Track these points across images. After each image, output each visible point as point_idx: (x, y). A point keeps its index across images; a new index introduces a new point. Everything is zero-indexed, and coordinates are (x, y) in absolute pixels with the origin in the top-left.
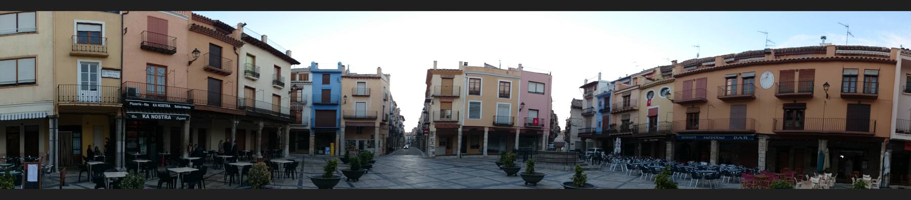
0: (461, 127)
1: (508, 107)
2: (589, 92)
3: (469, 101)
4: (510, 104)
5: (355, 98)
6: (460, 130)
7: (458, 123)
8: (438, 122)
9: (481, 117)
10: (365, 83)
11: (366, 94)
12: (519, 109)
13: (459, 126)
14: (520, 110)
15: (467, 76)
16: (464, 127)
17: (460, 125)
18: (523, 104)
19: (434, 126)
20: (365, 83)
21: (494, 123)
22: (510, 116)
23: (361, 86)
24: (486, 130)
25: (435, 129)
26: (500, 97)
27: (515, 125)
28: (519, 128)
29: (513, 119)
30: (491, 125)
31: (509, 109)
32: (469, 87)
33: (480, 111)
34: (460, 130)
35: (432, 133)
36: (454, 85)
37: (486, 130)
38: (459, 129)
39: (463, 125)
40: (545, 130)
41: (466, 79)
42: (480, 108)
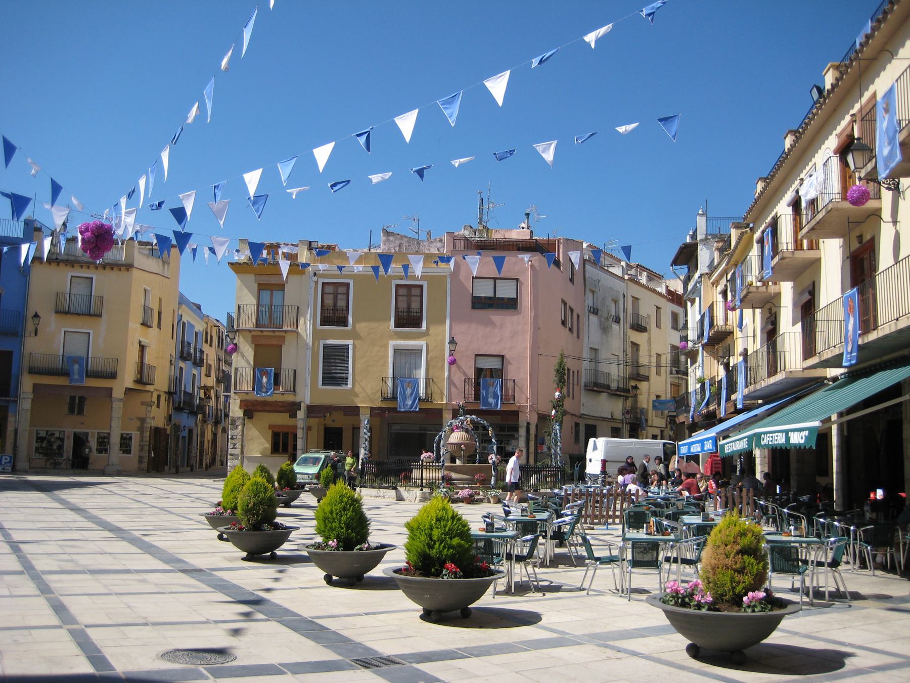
0: (303, 407)
15: (315, 279)
16: (312, 410)
17: (300, 403)
30: (378, 404)
39: (308, 402)
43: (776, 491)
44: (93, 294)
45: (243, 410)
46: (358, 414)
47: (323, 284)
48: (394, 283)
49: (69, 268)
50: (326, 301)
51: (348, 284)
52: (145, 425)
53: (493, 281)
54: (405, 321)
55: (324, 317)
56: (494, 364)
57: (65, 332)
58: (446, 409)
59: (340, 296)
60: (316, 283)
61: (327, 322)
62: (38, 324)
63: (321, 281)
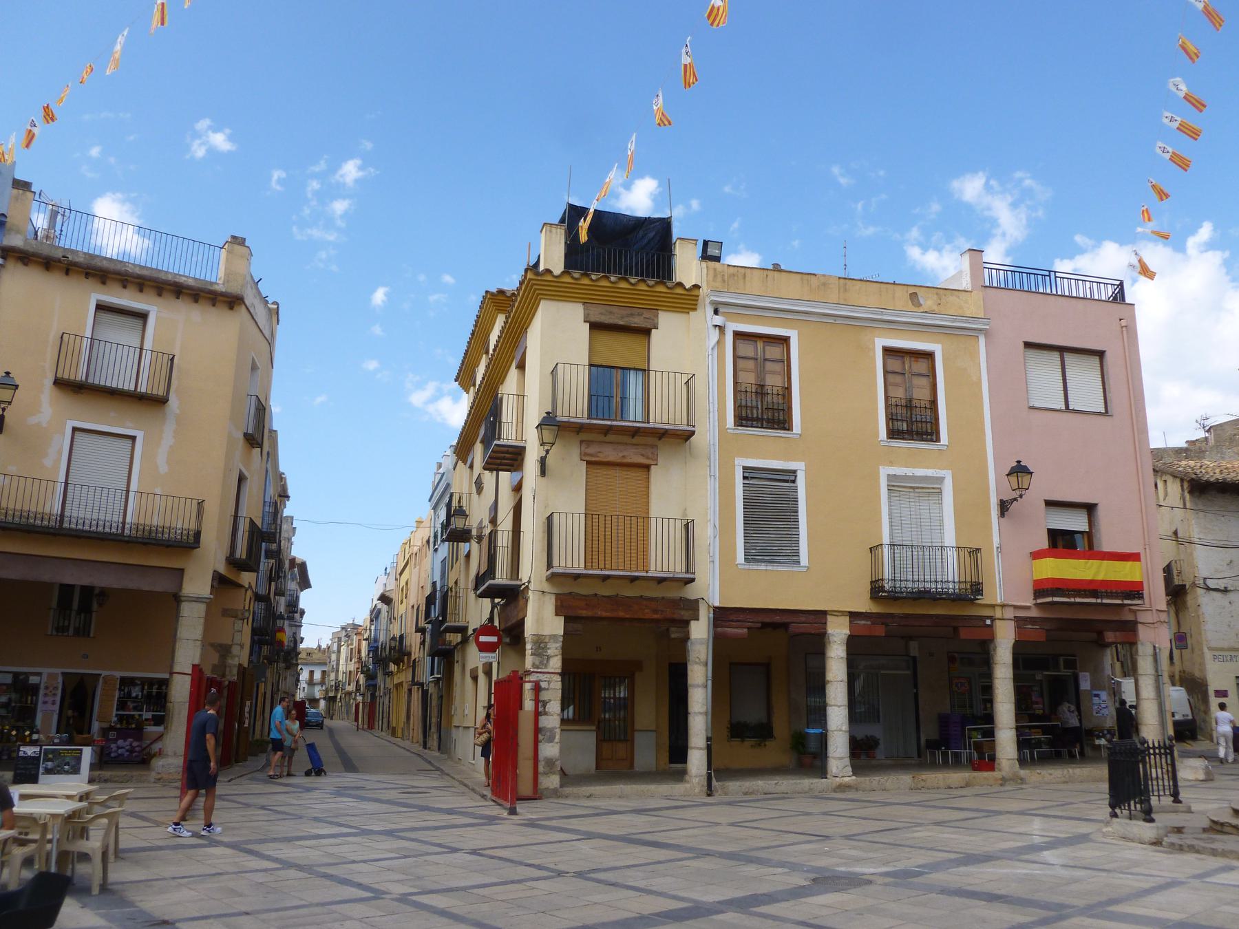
1: (929, 489)
3: (741, 462)
4: (948, 475)
5: (67, 402)
6: (700, 630)
7: (692, 592)
8: (577, 577)
10: (142, 316)
11: (142, 388)
13: (693, 607)
14: (1004, 507)
15: (718, 320)
16: (722, 615)
17: (697, 601)
18: (1020, 470)
19: (550, 604)
20: (142, 316)
21: (876, 590)
22: (950, 539)
23: (121, 334)
24: (838, 633)
25: (560, 621)
26: (893, 434)
27: (986, 599)
28: (1010, 614)
29: (976, 566)
30: (864, 605)
32: (736, 383)
34: (700, 630)
35: (540, 642)
37: (838, 633)
38: (693, 624)
40: (1142, 617)
41: (715, 336)
44: (148, 345)
45: (562, 618)
47: (738, 335)
48: (881, 342)
49: (89, 284)
51: (785, 341)
52: (230, 661)
53: (1056, 356)
55: (740, 406)
56: (1076, 522)
57: (75, 429)
61: (747, 419)
62: (10, 403)
63: (732, 327)
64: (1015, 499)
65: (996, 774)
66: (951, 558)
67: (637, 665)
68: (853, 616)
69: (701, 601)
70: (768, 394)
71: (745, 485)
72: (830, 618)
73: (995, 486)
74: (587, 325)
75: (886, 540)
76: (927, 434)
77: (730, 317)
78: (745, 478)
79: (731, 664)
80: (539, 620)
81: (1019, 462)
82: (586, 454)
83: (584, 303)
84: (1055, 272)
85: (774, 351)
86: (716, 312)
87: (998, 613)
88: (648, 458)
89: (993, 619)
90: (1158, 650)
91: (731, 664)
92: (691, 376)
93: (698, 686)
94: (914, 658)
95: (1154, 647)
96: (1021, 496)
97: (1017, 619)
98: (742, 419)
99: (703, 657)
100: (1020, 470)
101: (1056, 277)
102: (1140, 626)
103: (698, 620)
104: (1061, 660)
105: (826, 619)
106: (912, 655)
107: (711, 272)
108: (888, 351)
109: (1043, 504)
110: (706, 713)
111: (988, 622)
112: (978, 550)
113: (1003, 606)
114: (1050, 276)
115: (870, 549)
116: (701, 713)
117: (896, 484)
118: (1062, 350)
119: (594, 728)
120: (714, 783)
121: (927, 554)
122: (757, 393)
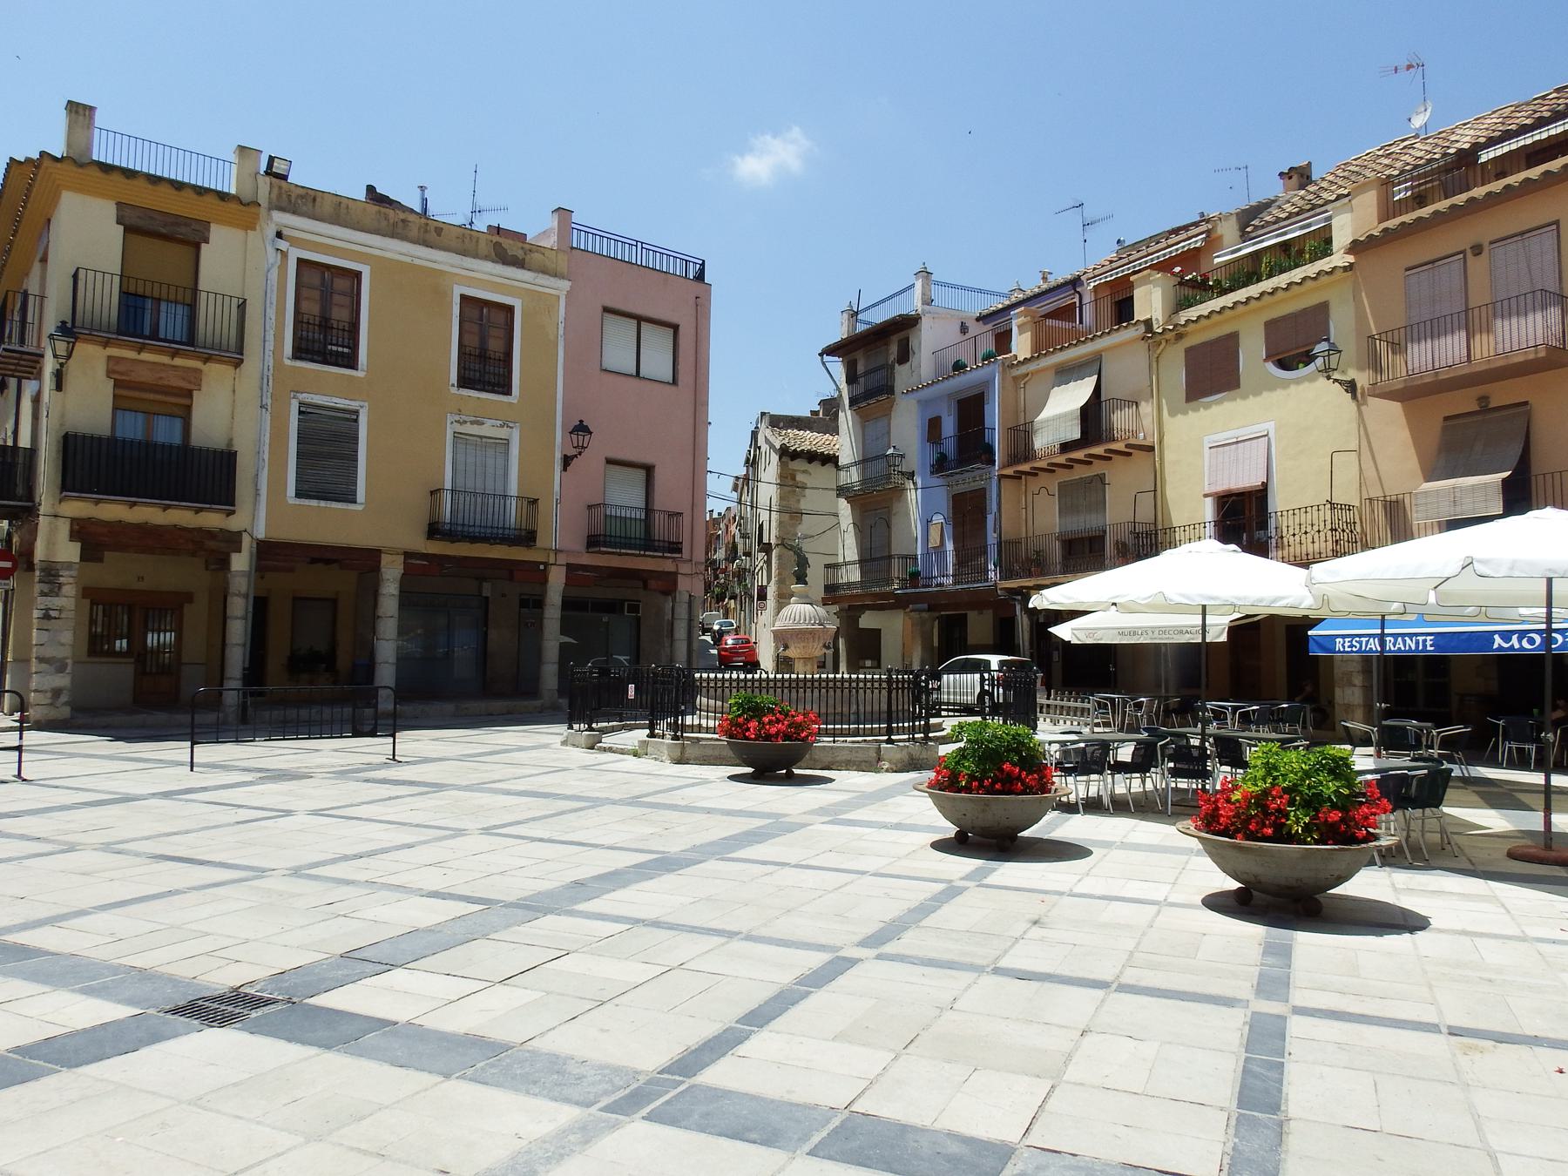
0: (246, 541)
2: (866, 373)
6: (240, 562)
9: (361, 494)
12: (558, 456)
14: (567, 461)
15: (283, 245)
16: (267, 551)
17: (239, 534)
18: (581, 428)
21: (434, 530)
22: (513, 489)
24: (392, 573)
26: (464, 382)
28: (562, 559)
31: (507, 453)
33: (354, 459)
34: (240, 562)
36: (203, 284)
37: (392, 573)
39: (261, 533)
42: (357, 439)
43: (636, 689)
45: (79, 544)
46: (376, 569)
47: (300, 261)
48: (458, 291)
50: (305, 306)
51: (358, 275)
54: (478, 374)
55: (301, 338)
58: (555, 564)
59: (337, 298)
60: (284, 255)
61: (307, 351)
63: (295, 254)
64: (576, 456)
65: (538, 703)
66: (513, 505)
67: (188, 597)
68: (408, 555)
69: (244, 533)
70: (333, 328)
71: (299, 420)
72: (383, 555)
73: (560, 441)
74: (121, 228)
75: (448, 485)
76: (498, 385)
77: (295, 242)
78: (300, 412)
79: (295, 599)
80: (51, 543)
81: (581, 421)
82: (114, 372)
83: (118, 204)
84: (642, 243)
85: (341, 284)
86: (279, 235)
87: (552, 560)
88: (190, 382)
89: (546, 564)
90: (692, 598)
91: (295, 599)
92: (241, 301)
93: (237, 618)
94: (487, 598)
95: (690, 596)
96: (580, 453)
97: (569, 566)
98: (300, 352)
99: (244, 589)
100: (581, 428)
101: (642, 248)
102: (680, 578)
103: (240, 552)
104: (626, 604)
105: (380, 556)
106: (484, 595)
107: (275, 191)
108: (464, 298)
109: (604, 461)
110: (244, 645)
111: (542, 567)
112: (535, 501)
113: (557, 551)
114: (636, 246)
115: (432, 492)
116: (239, 645)
117: (457, 436)
118: (640, 319)
119: (132, 660)
120: (250, 711)
121: (479, 500)
122: (320, 326)
